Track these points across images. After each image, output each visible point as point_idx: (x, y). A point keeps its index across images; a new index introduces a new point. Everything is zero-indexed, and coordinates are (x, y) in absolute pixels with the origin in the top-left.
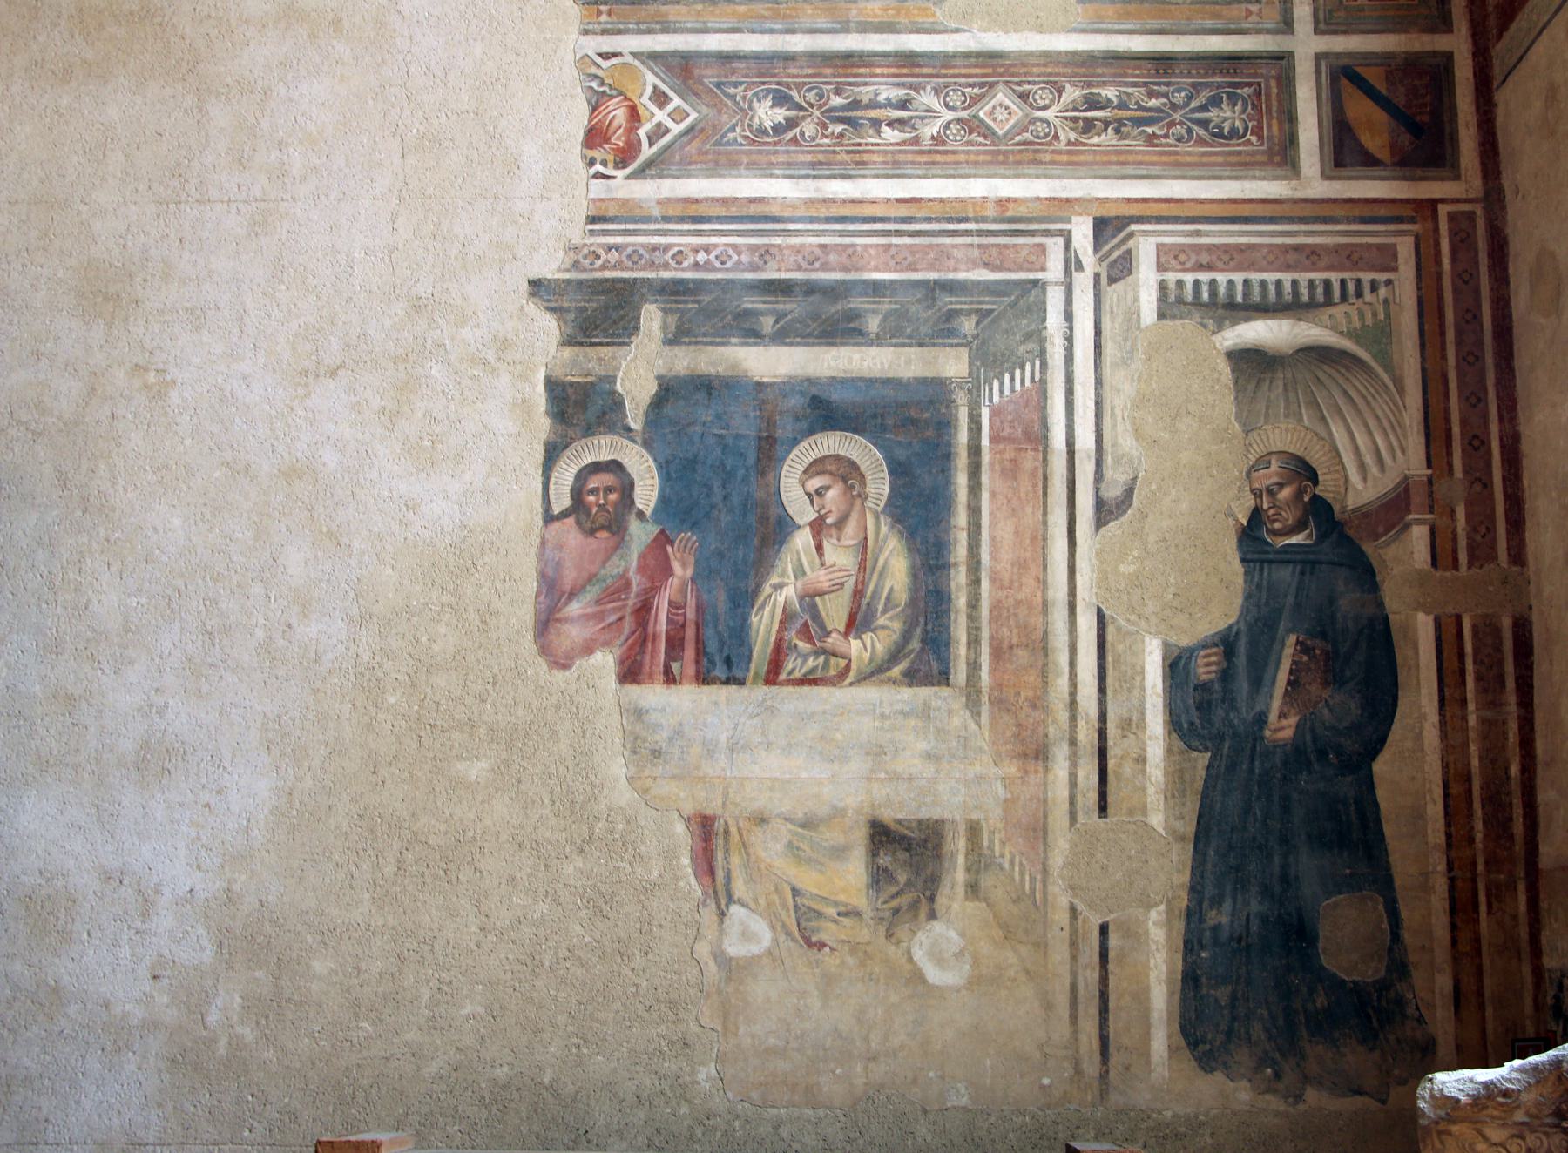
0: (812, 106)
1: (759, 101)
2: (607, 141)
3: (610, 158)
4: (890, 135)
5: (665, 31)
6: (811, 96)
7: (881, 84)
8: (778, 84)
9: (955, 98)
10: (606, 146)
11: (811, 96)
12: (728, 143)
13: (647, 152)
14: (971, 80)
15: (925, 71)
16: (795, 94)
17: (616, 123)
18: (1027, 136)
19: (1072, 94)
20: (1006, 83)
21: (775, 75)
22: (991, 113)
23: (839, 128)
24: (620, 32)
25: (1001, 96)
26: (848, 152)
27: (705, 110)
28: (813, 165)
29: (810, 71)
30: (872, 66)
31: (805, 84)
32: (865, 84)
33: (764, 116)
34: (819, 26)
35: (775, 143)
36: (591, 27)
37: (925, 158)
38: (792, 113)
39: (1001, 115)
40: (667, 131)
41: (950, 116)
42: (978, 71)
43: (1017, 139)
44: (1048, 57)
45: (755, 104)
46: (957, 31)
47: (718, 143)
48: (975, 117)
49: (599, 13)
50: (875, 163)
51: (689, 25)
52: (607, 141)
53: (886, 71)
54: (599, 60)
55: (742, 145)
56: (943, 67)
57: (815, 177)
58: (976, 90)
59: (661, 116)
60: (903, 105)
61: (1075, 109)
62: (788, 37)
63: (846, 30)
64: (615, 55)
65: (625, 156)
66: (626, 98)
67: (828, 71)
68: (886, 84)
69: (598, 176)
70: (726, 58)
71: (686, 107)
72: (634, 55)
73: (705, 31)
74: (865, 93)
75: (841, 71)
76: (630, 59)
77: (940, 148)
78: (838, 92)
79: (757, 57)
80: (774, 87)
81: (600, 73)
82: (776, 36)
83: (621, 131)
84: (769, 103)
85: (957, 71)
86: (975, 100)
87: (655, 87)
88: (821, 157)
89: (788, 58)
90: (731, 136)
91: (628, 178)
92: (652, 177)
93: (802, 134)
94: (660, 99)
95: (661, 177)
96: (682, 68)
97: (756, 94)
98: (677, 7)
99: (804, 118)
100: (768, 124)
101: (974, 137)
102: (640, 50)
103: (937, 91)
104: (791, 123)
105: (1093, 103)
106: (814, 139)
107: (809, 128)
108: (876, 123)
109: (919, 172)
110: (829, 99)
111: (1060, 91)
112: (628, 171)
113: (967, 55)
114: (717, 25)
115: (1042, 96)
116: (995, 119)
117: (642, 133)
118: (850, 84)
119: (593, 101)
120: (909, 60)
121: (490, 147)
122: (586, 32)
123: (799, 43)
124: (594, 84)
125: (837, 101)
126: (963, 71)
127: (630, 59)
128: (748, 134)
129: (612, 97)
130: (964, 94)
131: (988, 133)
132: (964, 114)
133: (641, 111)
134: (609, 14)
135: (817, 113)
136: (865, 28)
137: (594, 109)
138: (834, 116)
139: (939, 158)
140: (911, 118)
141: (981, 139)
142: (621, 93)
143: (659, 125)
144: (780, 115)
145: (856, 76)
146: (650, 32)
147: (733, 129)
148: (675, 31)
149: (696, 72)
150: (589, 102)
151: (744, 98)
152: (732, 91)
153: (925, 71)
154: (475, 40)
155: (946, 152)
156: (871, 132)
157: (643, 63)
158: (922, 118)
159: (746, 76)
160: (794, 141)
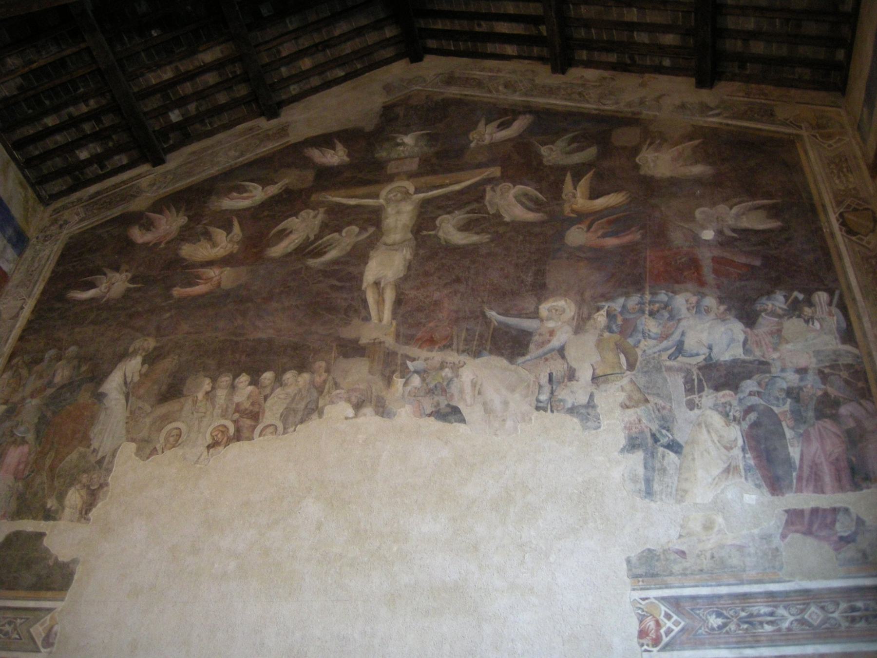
0: (732, 617)
1: (710, 616)
2: (647, 635)
3: (650, 643)
4: (768, 628)
5: (668, 586)
6: (732, 613)
7: (760, 606)
8: (717, 608)
9: (793, 611)
10: (648, 638)
11: (732, 613)
12: (699, 635)
13: (665, 640)
14: (799, 602)
15: (779, 599)
16: (724, 612)
17: (651, 628)
18: (827, 625)
19: (843, 606)
20: (814, 602)
21: (715, 604)
22: (810, 616)
23: (746, 626)
24: (648, 589)
25: (813, 609)
26: (752, 636)
27: (687, 620)
28: (738, 643)
29: (730, 602)
30: (756, 598)
31: (728, 608)
32: (754, 606)
33: (713, 622)
34: (731, 582)
35: (719, 634)
36: (636, 587)
37: (783, 638)
38: (724, 620)
39: (815, 617)
40: (673, 630)
41: (792, 618)
42: (799, 598)
43: (823, 626)
44: (831, 591)
45: (709, 617)
46: (789, 581)
47: (695, 635)
48: (803, 618)
49: (639, 582)
50: (762, 641)
51: (677, 585)
52: (647, 635)
53: (762, 600)
54: (641, 601)
55: (704, 635)
56: (786, 597)
57: (738, 648)
58: (801, 607)
59: (669, 624)
60: (772, 614)
61: (846, 612)
62: (719, 588)
63: (742, 583)
64: (647, 599)
65: (656, 642)
66: (654, 617)
67: (738, 601)
68: (762, 606)
69: (646, 651)
70: (693, 598)
71: (679, 619)
72: (656, 598)
73: (684, 587)
74: (754, 610)
75: (743, 601)
76: (654, 600)
77: (790, 632)
78: (743, 610)
79: (707, 597)
80: (715, 609)
81: (641, 606)
82: (713, 588)
83: (653, 632)
84: (714, 616)
85: (792, 598)
86: (803, 611)
87: (665, 612)
88: (739, 639)
89: (720, 597)
90: (700, 631)
91: (659, 651)
92: (669, 651)
93: (730, 629)
94: (668, 617)
95: (673, 650)
96: (676, 603)
97: (708, 613)
98: (671, 577)
99: (730, 622)
100: (715, 626)
101: (804, 627)
102: (657, 596)
103: (785, 607)
104: (725, 625)
105: (853, 609)
106: (735, 631)
107: (733, 627)
108: (761, 623)
109: (783, 644)
110: (739, 614)
111: (838, 604)
112: (658, 648)
113: (796, 591)
114: (688, 584)
115: (831, 607)
116: (812, 619)
117: (662, 631)
118: (748, 607)
119: (640, 619)
120: (771, 595)
121: (599, 639)
122: (634, 590)
123: (723, 590)
124: (640, 611)
125: (743, 614)
126: (795, 598)
127: (654, 600)
128: (707, 630)
129: (648, 617)
130: (796, 608)
131: (810, 625)
132: (798, 617)
133: (661, 622)
134: (643, 581)
135: (735, 620)
136: (751, 582)
137: (641, 622)
138: (743, 621)
139: (790, 637)
140: (776, 620)
141: (807, 628)
142: (651, 615)
143: (669, 628)
144: (720, 621)
145: (749, 603)
146: (660, 588)
147: (700, 628)
148: (671, 587)
149: (682, 604)
150: (638, 619)
151: (703, 615)
152: (698, 612)
153: (779, 599)
154: (589, 595)
155: (792, 634)
156: (759, 627)
157: (659, 601)
158: (780, 620)
159: (703, 605)
160: (727, 633)
